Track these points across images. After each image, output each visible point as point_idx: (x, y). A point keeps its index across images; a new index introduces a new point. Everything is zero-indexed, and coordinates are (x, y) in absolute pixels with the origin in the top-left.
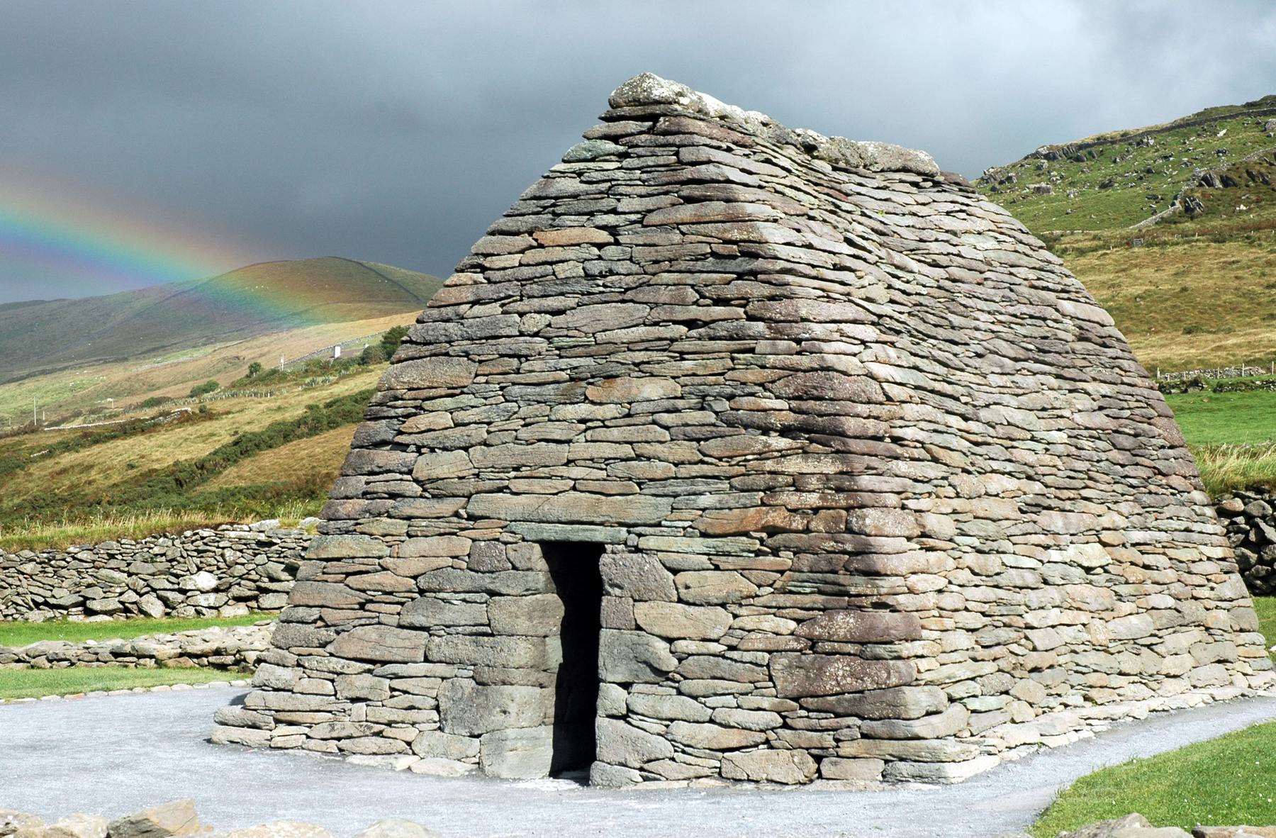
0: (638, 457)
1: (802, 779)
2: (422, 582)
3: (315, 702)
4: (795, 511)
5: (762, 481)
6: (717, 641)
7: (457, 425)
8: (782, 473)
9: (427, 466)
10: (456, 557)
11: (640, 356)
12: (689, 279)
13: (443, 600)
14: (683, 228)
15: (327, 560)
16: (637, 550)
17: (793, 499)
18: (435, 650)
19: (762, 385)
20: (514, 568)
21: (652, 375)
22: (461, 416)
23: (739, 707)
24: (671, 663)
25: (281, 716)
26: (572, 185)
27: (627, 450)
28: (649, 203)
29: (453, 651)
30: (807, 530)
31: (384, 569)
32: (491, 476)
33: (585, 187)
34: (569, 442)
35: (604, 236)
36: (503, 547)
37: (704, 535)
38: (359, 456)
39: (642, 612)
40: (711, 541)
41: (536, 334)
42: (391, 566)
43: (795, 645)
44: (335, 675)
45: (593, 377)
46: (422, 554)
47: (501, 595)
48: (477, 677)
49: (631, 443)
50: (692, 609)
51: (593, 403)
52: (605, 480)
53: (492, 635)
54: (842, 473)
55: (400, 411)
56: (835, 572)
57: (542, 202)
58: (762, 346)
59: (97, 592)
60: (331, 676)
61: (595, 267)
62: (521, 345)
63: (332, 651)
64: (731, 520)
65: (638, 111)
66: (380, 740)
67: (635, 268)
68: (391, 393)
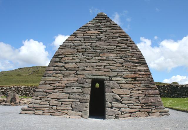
0: (110, 66)
1: (146, 116)
2: (67, 85)
3: (45, 106)
5: (134, 70)
6: (129, 95)
7: (73, 59)
8: (137, 69)
9: (67, 66)
10: (75, 81)
11: (109, 50)
12: (116, 40)
13: (72, 88)
14: (114, 33)
15: (46, 81)
17: (140, 73)
18: (71, 97)
19: (131, 56)
20: (87, 83)
21: (112, 53)
23: (134, 105)
25: (37, 109)
26: (92, 25)
27: (108, 64)
30: (142, 78)
31: (59, 83)
33: (94, 26)
34: (96, 63)
35: (99, 33)
37: (124, 78)
38: (53, 64)
39: (114, 90)
40: (126, 79)
41: (89, 46)
43: (143, 95)
44: (49, 101)
47: (85, 87)
49: (109, 63)
51: (101, 57)
53: (83, 94)
54: (147, 69)
56: (148, 84)
57: (87, 27)
58: (130, 50)
60: (48, 101)
61: (99, 37)
62: (86, 47)
63: (48, 97)
64: (130, 76)
65: (103, 16)
66: (60, 113)
67: (106, 37)
68: (59, 54)
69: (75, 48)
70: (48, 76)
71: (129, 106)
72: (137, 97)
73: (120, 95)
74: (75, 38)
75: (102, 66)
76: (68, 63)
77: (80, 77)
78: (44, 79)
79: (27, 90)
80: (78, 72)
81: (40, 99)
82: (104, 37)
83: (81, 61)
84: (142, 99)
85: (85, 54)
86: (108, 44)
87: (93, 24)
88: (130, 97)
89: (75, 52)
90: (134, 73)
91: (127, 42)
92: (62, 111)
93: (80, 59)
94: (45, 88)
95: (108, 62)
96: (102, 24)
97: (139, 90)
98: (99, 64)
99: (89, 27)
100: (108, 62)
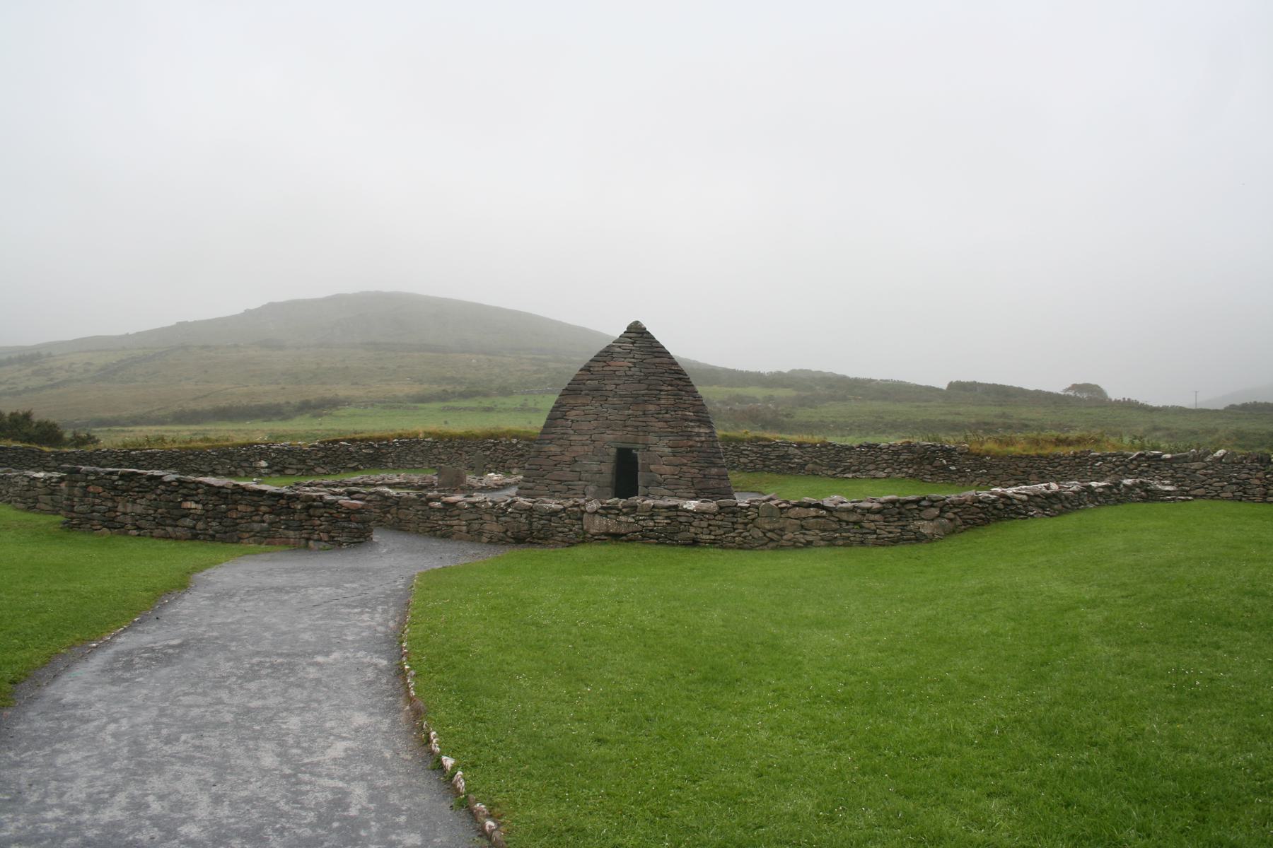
4: (697, 442)
5: (687, 434)
11: (646, 398)
16: (648, 451)
17: (697, 439)
26: (618, 350)
27: (644, 424)
28: (644, 357)
39: (652, 467)
58: (684, 398)
59: (219, 467)
62: (606, 393)
65: (639, 331)
72: (690, 479)
79: (440, 450)
84: (699, 482)
86: (646, 386)
87: (620, 347)
91: (679, 382)
95: (645, 419)
97: (694, 467)
98: (628, 423)
100: (645, 419)
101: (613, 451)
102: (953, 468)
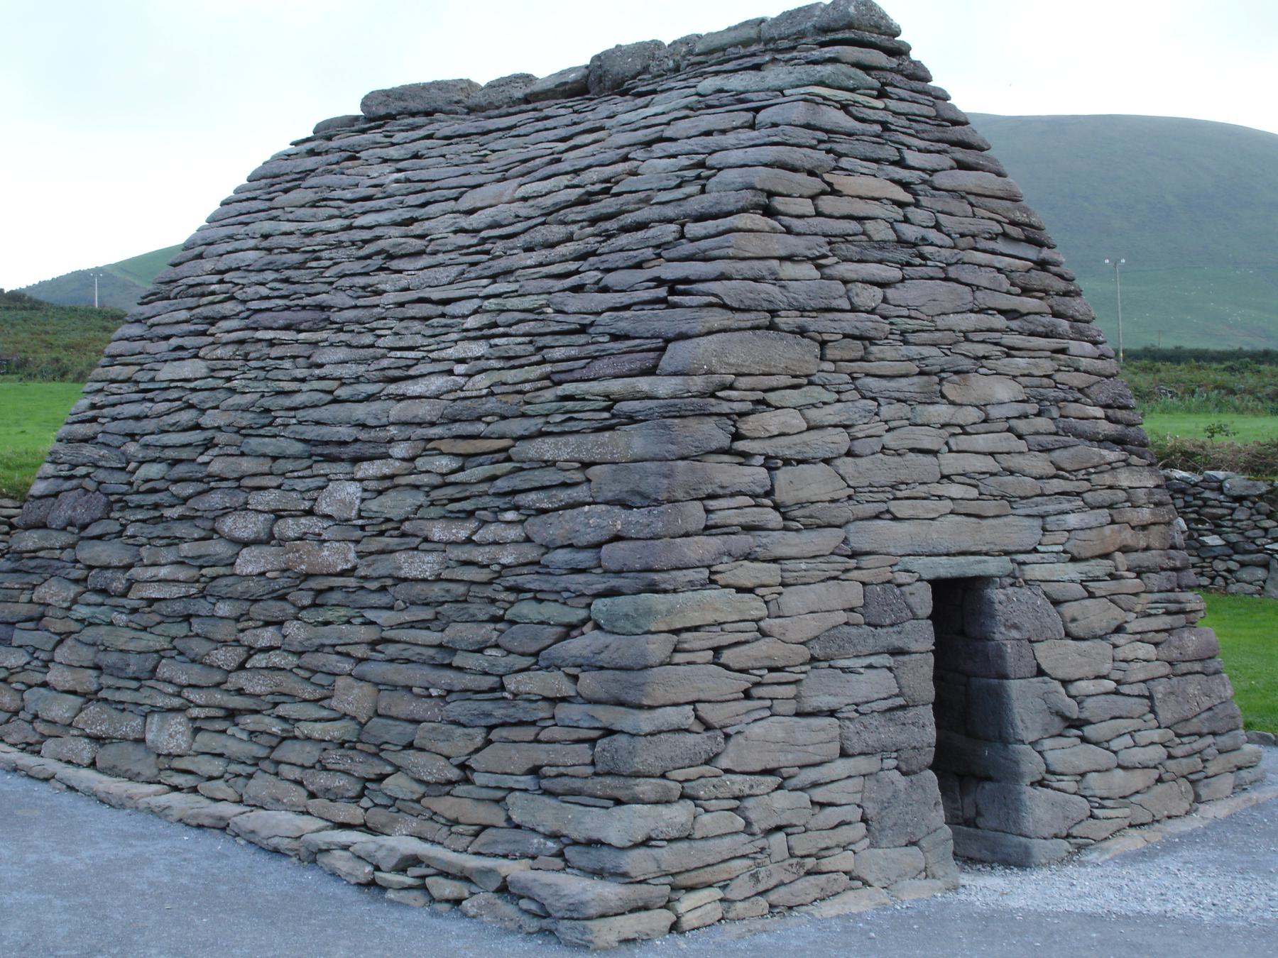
5: (1106, 496)
7: (809, 429)
10: (852, 610)
11: (981, 350)
13: (843, 670)
14: (972, 199)
15: (676, 632)
22: (815, 415)
24: (1072, 710)
27: (988, 464)
29: (875, 736)
31: (764, 634)
32: (868, 496)
36: (897, 591)
37: (1074, 559)
40: (1082, 566)
42: (776, 631)
45: (943, 371)
46: (811, 610)
48: (904, 768)
50: (1083, 645)
51: (952, 403)
52: (978, 499)
55: (738, 407)
56: (1172, 590)
61: (910, 232)
67: (948, 241)
68: (716, 378)
69: (802, 332)
70: (693, 586)
71: (1121, 754)
73: (1071, 682)
74: (774, 231)
75: (969, 479)
76: (787, 462)
77: (873, 569)
78: (669, 612)
80: (859, 543)
81: (683, 796)
82: (933, 235)
83: (858, 447)
85: (872, 383)
87: (844, 107)
88: (1116, 692)
89: (811, 365)
90: (1113, 522)
92: (826, 864)
93: (846, 427)
94: (690, 699)
96: (895, 113)
97: (1141, 636)
98: (950, 463)
99: (827, 131)
101: (923, 599)
102: (1213, 540)
